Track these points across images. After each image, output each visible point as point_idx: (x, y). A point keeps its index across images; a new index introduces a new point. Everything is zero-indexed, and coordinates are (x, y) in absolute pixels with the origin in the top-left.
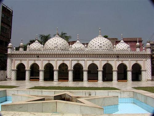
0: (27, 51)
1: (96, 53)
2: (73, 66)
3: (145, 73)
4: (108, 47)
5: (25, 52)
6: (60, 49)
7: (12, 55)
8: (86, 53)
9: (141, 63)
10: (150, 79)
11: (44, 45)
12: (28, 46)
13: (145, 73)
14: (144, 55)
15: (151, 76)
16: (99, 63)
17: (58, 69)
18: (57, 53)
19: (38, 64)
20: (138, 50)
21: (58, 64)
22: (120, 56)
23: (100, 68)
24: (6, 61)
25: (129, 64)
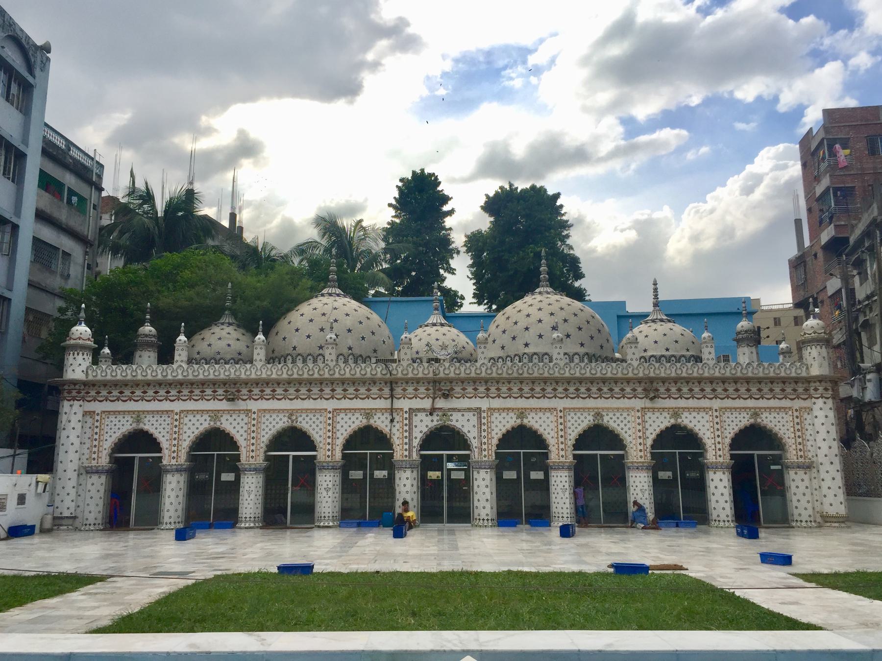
0: (175, 366)
1: (536, 375)
2: (416, 443)
3: (806, 477)
4: (587, 341)
5: (159, 372)
6: (345, 351)
7: (86, 389)
8: (483, 374)
9: (778, 422)
10: (842, 510)
11: (266, 334)
12: (182, 338)
13: (806, 477)
14: (796, 380)
15: (841, 497)
16: (553, 426)
17: (338, 455)
18: (337, 376)
19: (233, 432)
20: (744, 355)
21: (338, 434)
22: (662, 390)
23: (560, 451)
24: (55, 414)
25: (715, 426)
